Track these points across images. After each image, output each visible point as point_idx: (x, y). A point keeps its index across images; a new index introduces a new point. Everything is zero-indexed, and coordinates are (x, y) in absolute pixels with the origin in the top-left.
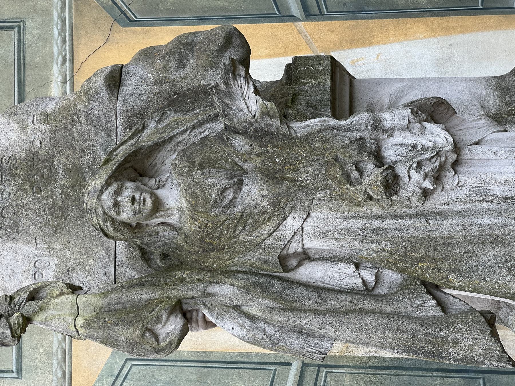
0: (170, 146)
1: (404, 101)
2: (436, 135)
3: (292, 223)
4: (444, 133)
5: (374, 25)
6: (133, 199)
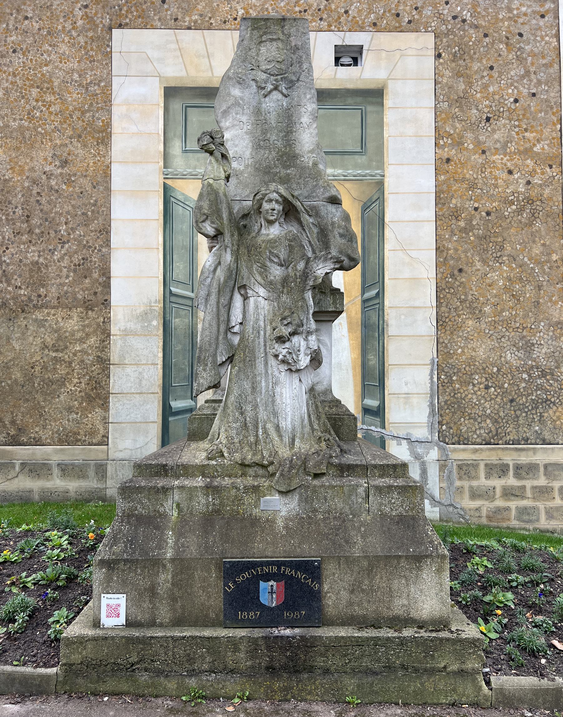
0: (300, 229)
1: (321, 346)
2: (304, 361)
3: (262, 291)
4: (305, 365)
5: (358, 334)
6: (274, 210)
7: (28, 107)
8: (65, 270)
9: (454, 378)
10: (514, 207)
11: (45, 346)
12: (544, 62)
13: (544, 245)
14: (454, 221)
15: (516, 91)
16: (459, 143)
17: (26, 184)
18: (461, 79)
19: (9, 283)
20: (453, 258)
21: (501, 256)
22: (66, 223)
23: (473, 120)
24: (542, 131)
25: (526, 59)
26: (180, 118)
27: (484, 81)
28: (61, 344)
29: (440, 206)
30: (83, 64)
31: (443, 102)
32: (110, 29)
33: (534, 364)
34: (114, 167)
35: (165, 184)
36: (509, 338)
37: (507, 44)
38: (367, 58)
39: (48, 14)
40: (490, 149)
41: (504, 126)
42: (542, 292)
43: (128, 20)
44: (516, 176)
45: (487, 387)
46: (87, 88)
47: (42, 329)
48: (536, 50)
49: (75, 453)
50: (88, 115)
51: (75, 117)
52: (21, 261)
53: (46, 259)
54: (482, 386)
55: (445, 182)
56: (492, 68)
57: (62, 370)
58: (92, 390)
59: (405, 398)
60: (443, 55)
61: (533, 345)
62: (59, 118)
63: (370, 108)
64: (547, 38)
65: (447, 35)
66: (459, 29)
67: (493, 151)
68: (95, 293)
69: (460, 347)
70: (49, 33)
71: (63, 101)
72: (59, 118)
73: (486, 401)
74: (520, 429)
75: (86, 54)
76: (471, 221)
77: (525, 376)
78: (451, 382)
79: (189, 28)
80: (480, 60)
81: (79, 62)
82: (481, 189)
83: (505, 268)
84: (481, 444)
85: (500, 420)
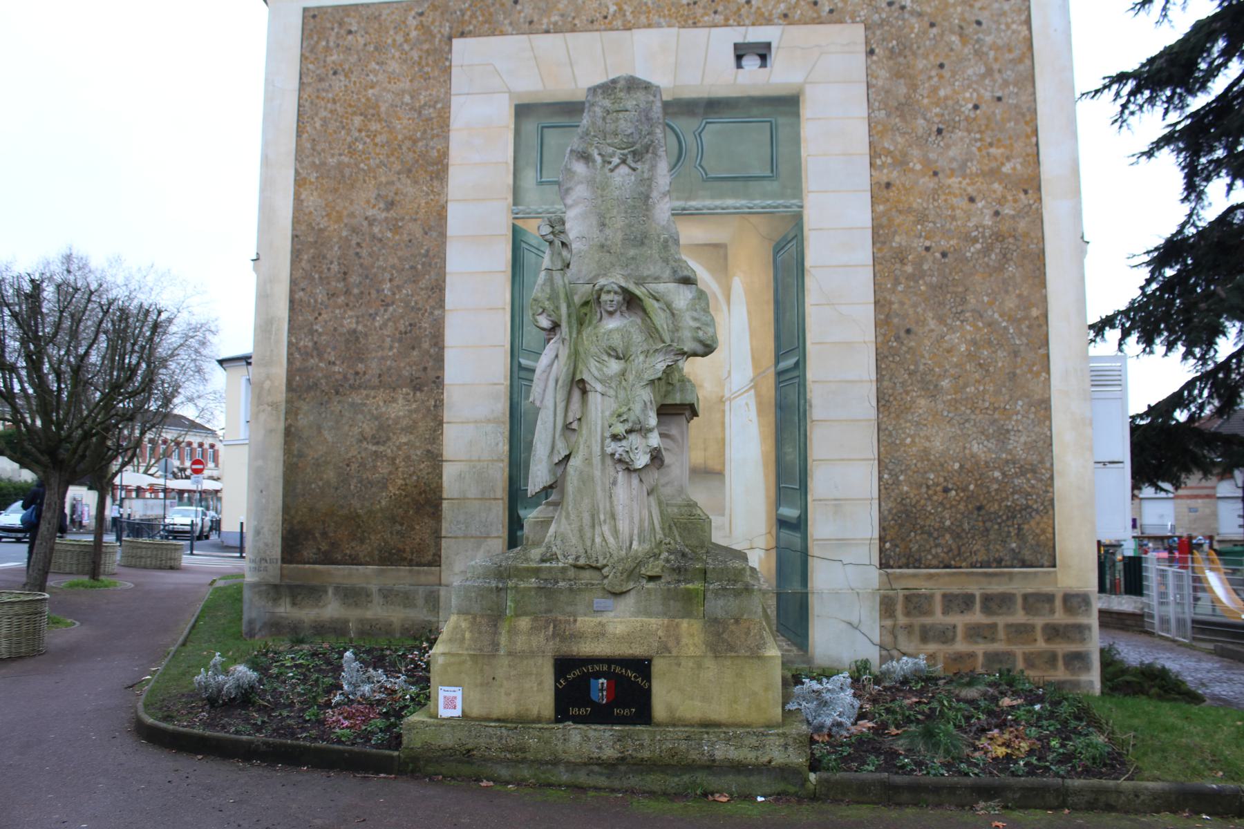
2: (642, 460)
4: (643, 464)
7: (349, 139)
8: (388, 340)
9: (902, 478)
10: (978, 246)
11: (363, 438)
12: (1011, 56)
13: (1019, 296)
14: (898, 266)
15: (975, 95)
16: (901, 162)
17: (344, 234)
18: (902, 81)
19: (321, 358)
20: (898, 315)
21: (962, 311)
22: (391, 280)
23: (920, 132)
24: (1011, 145)
25: (987, 54)
26: (535, 141)
27: (932, 83)
28: (382, 434)
29: (878, 245)
30: (416, 84)
31: (879, 109)
32: (450, 39)
33: (1009, 457)
34: (450, 205)
35: (514, 226)
36: (975, 425)
37: (961, 36)
38: (776, 57)
39: (376, 26)
40: (943, 171)
41: (962, 139)
42: (1019, 360)
43: (471, 27)
44: (980, 205)
45: (946, 490)
46: (420, 113)
47: (360, 416)
48: (1000, 42)
49: (399, 577)
50: (420, 144)
51: (404, 148)
52: (335, 329)
53: (365, 326)
54: (939, 488)
55: (884, 214)
56: (941, 66)
57: (384, 469)
58: (420, 494)
59: (835, 505)
60: (877, 51)
61: (1008, 431)
62: (386, 150)
63: (782, 120)
64: (1014, 26)
65: (881, 25)
66: (897, 18)
67: (948, 172)
68: (425, 369)
69: (909, 435)
70: (376, 49)
71: (391, 130)
72: (386, 150)
73: (945, 508)
74: (991, 547)
75: (420, 70)
76: (921, 264)
77: (997, 474)
78: (897, 483)
79: (547, 32)
80: (926, 56)
81: (411, 81)
82: (934, 223)
83: (968, 328)
84: (938, 567)
85: (963, 535)
